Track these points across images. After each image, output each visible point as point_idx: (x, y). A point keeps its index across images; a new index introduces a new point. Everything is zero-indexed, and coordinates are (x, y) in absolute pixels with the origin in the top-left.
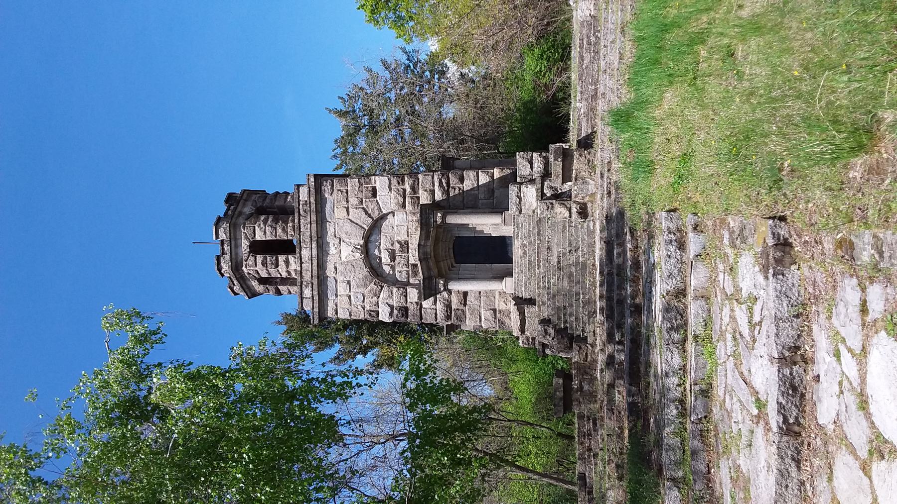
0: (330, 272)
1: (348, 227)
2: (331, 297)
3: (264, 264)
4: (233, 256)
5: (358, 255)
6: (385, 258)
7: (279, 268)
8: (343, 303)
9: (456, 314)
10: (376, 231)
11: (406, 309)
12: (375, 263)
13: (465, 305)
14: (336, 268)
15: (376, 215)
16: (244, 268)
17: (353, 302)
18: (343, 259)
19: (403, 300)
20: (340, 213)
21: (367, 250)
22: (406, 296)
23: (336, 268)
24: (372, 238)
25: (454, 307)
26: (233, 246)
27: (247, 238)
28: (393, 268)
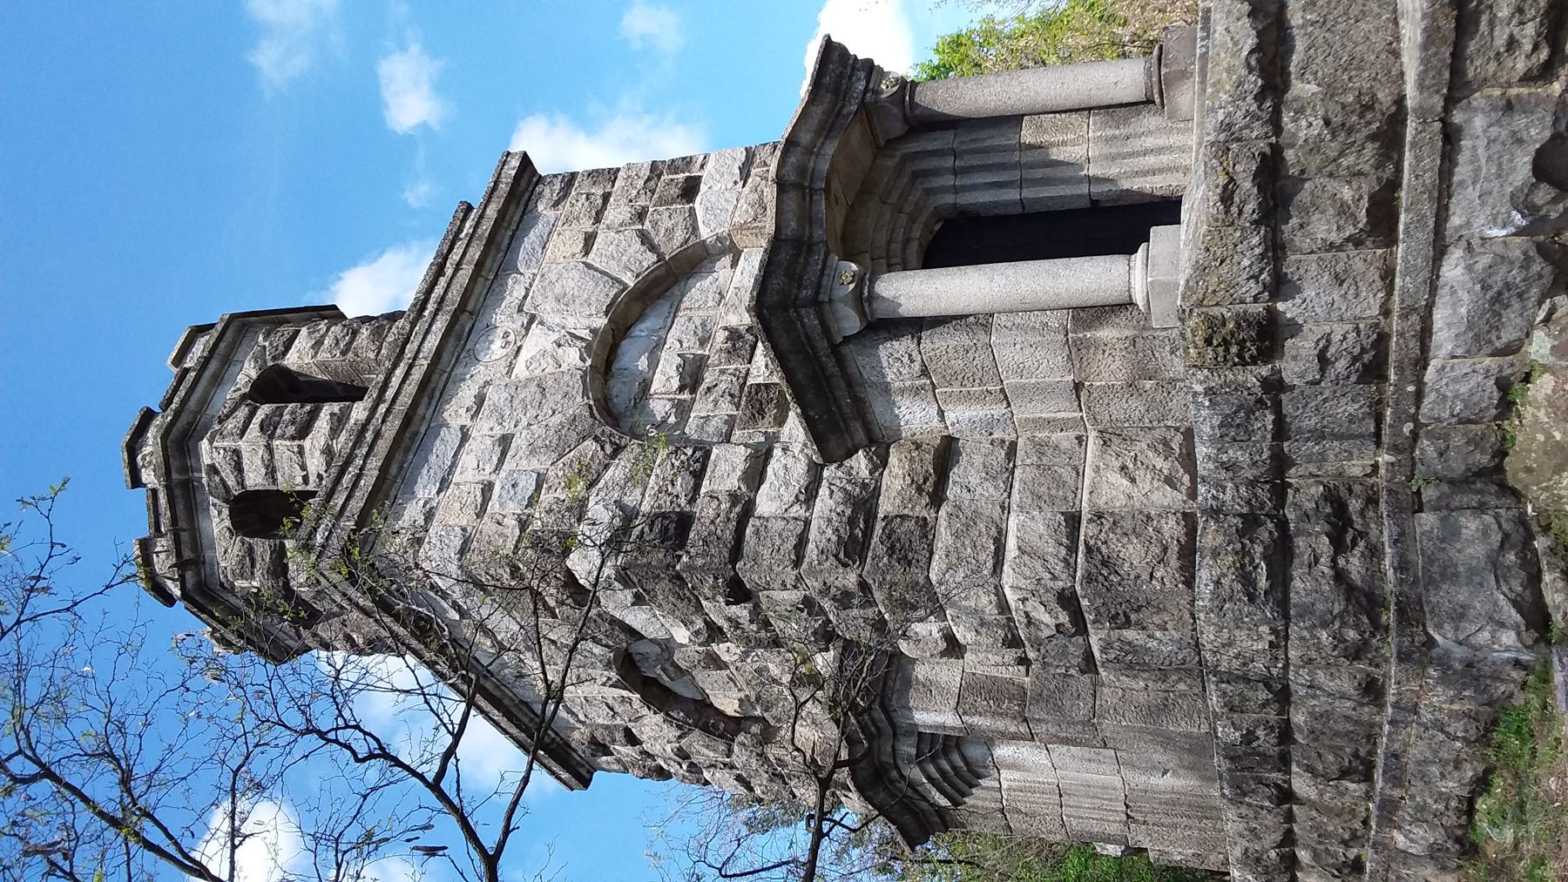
0: (456, 413)
1: (574, 281)
2: (425, 489)
3: (269, 428)
4: (192, 404)
5: (572, 356)
6: (665, 379)
7: (307, 443)
8: (455, 514)
9: (889, 534)
10: (664, 307)
11: (684, 521)
12: (621, 392)
13: (937, 499)
14: (480, 400)
15: (671, 248)
16: (204, 444)
17: (494, 506)
18: (520, 370)
19: (681, 485)
20: (566, 244)
21: (606, 352)
22: (698, 476)
23: (480, 400)
24: (642, 329)
25: (886, 506)
26: (208, 374)
27: (260, 357)
28: (683, 410)
